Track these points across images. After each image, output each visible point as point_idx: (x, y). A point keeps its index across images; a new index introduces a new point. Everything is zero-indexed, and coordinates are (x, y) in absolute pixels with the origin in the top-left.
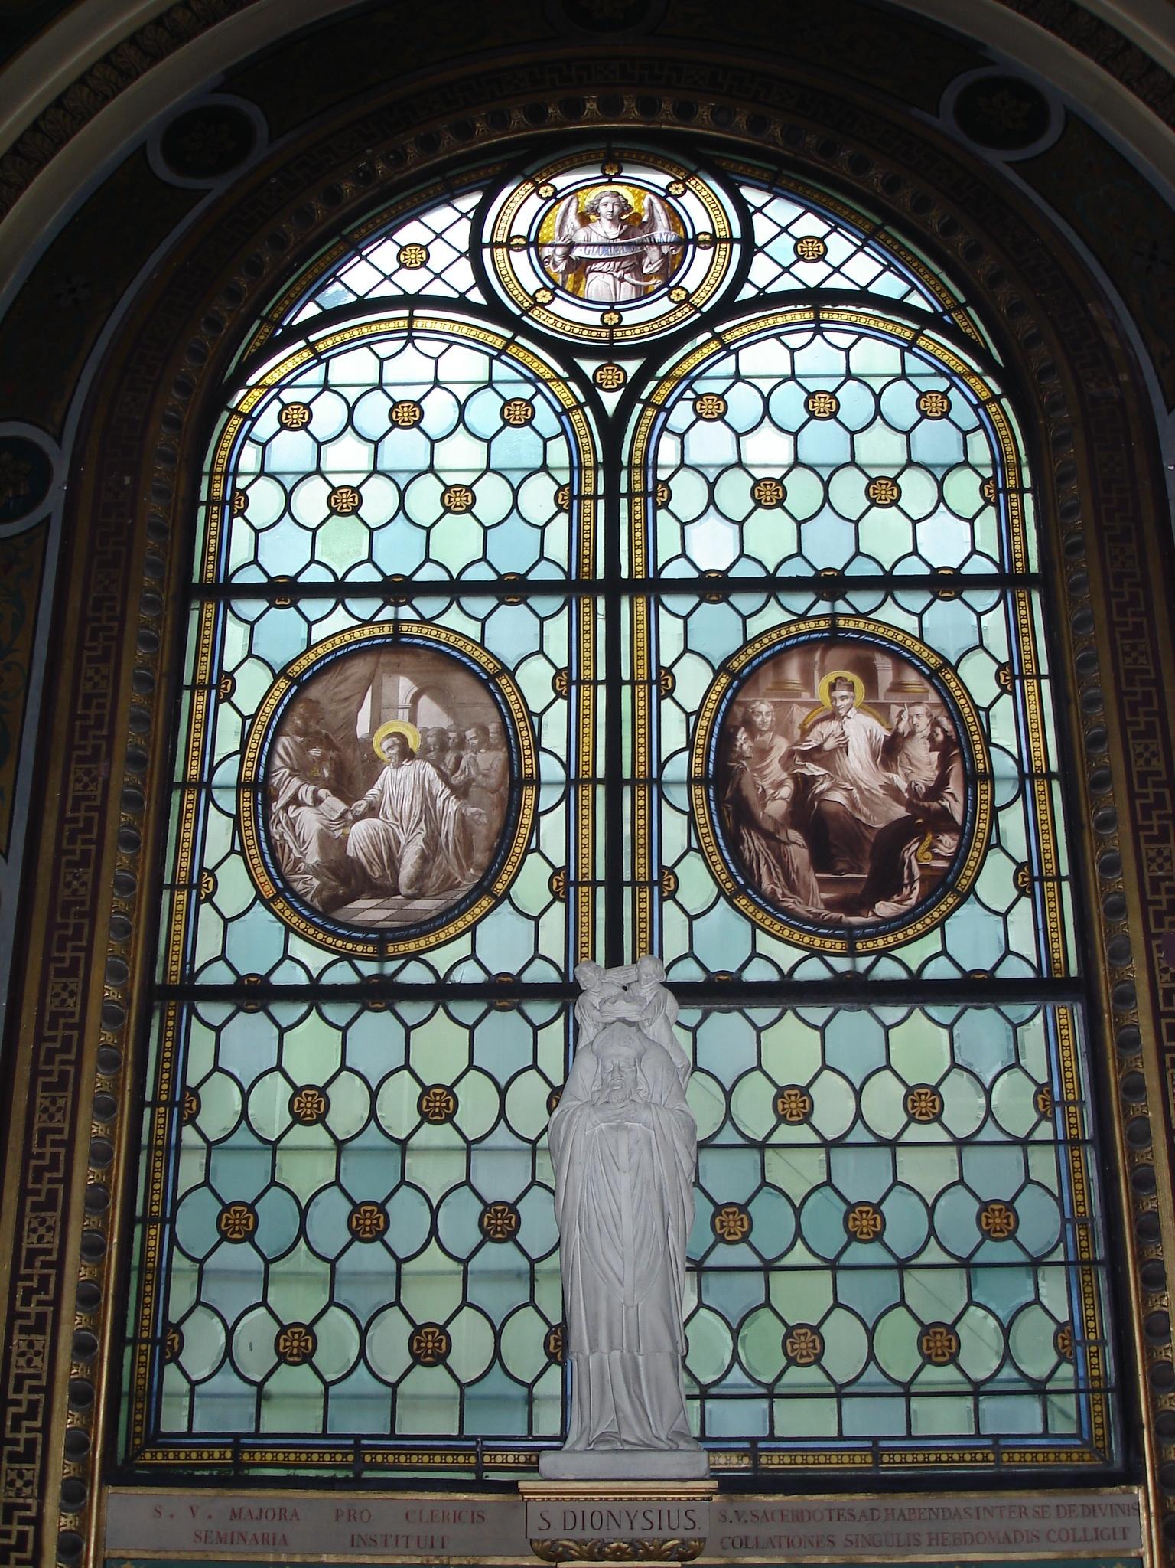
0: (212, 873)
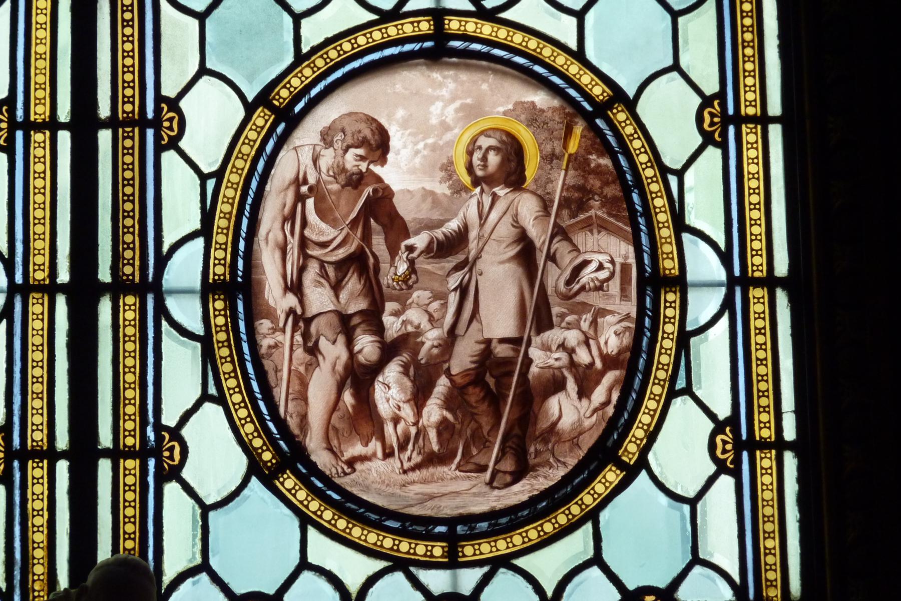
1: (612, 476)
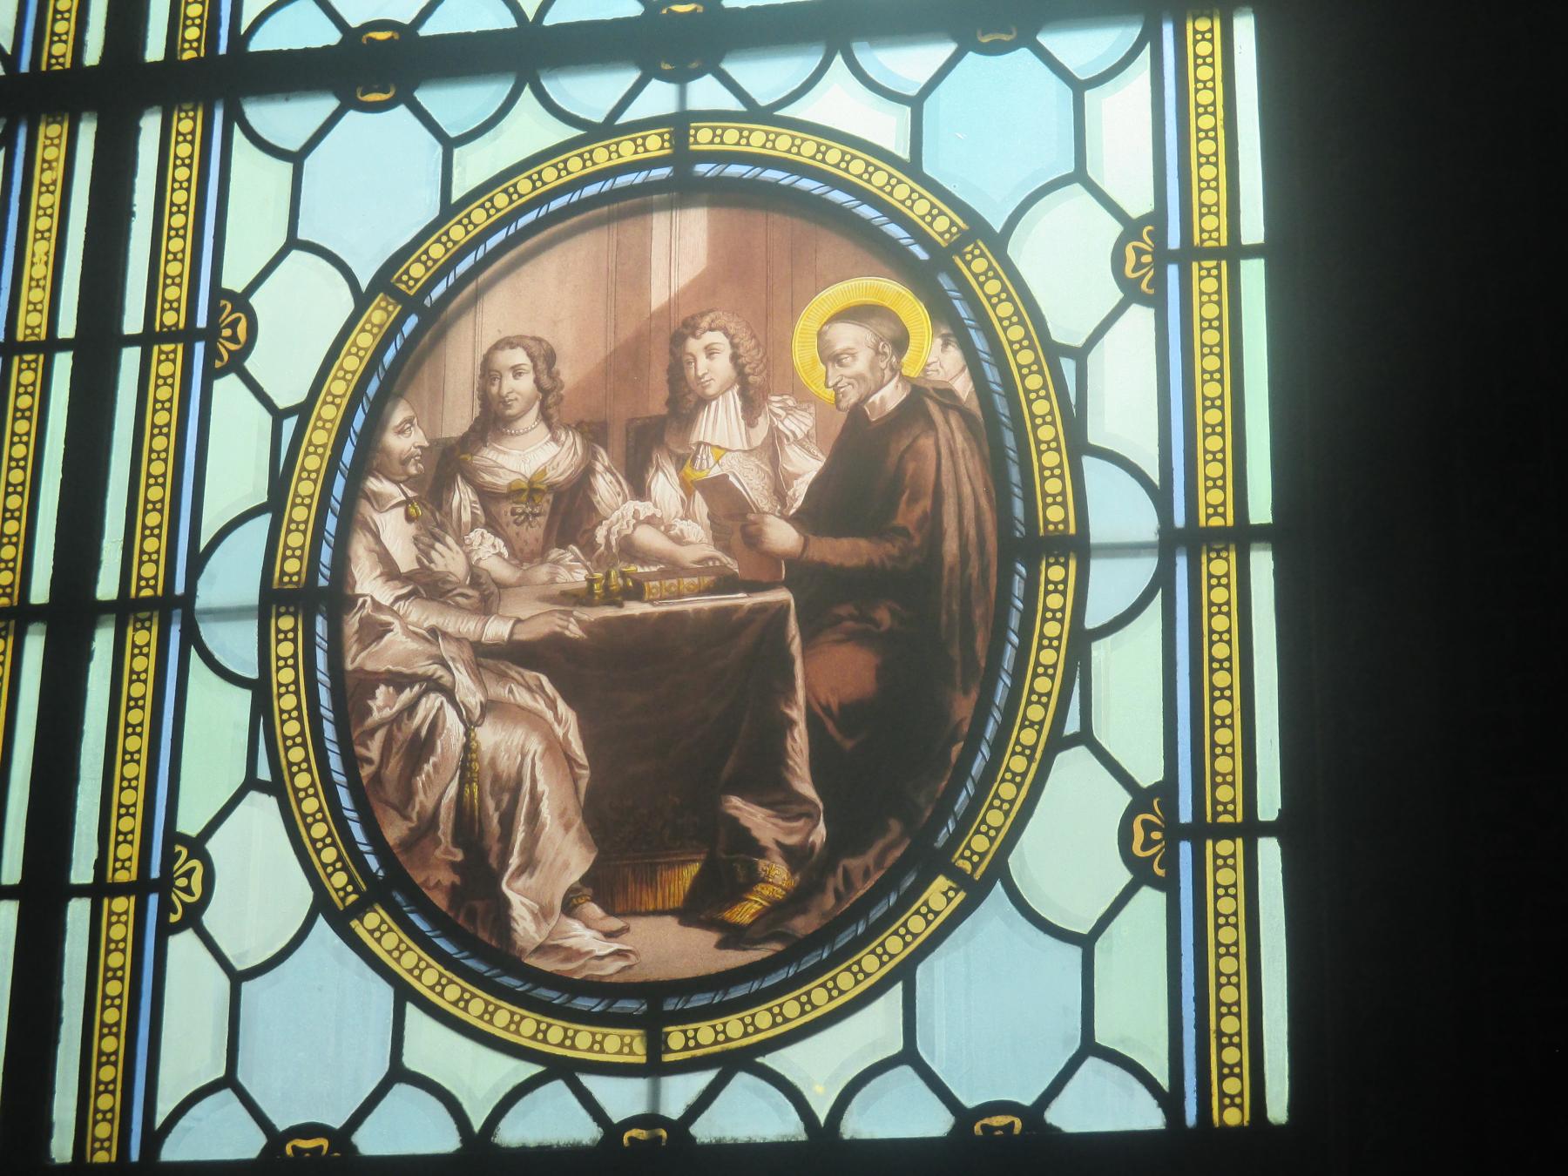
0: (197, 847)
1: (939, 894)
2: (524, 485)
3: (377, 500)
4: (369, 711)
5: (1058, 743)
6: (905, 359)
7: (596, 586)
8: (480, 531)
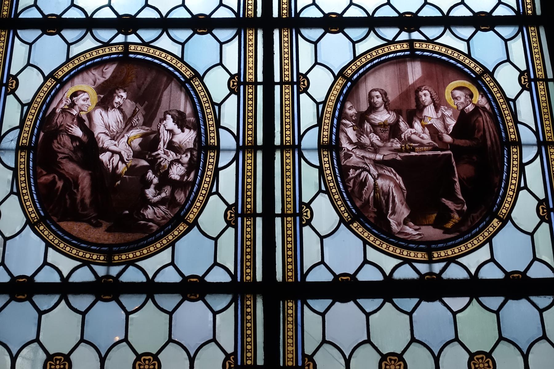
0: (308, 205)
2: (382, 123)
3: (345, 125)
4: (349, 175)
5: (519, 189)
6: (473, 99)
7: (403, 148)
8: (372, 134)
